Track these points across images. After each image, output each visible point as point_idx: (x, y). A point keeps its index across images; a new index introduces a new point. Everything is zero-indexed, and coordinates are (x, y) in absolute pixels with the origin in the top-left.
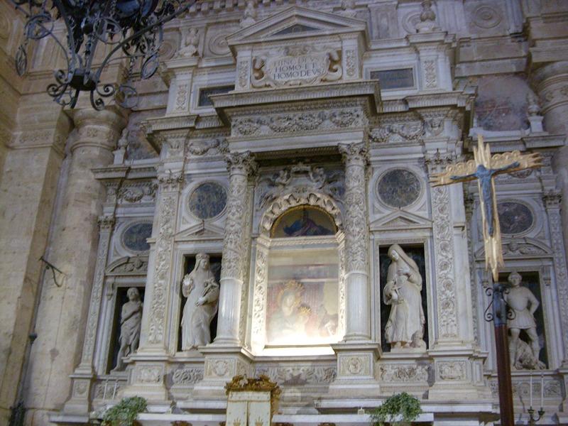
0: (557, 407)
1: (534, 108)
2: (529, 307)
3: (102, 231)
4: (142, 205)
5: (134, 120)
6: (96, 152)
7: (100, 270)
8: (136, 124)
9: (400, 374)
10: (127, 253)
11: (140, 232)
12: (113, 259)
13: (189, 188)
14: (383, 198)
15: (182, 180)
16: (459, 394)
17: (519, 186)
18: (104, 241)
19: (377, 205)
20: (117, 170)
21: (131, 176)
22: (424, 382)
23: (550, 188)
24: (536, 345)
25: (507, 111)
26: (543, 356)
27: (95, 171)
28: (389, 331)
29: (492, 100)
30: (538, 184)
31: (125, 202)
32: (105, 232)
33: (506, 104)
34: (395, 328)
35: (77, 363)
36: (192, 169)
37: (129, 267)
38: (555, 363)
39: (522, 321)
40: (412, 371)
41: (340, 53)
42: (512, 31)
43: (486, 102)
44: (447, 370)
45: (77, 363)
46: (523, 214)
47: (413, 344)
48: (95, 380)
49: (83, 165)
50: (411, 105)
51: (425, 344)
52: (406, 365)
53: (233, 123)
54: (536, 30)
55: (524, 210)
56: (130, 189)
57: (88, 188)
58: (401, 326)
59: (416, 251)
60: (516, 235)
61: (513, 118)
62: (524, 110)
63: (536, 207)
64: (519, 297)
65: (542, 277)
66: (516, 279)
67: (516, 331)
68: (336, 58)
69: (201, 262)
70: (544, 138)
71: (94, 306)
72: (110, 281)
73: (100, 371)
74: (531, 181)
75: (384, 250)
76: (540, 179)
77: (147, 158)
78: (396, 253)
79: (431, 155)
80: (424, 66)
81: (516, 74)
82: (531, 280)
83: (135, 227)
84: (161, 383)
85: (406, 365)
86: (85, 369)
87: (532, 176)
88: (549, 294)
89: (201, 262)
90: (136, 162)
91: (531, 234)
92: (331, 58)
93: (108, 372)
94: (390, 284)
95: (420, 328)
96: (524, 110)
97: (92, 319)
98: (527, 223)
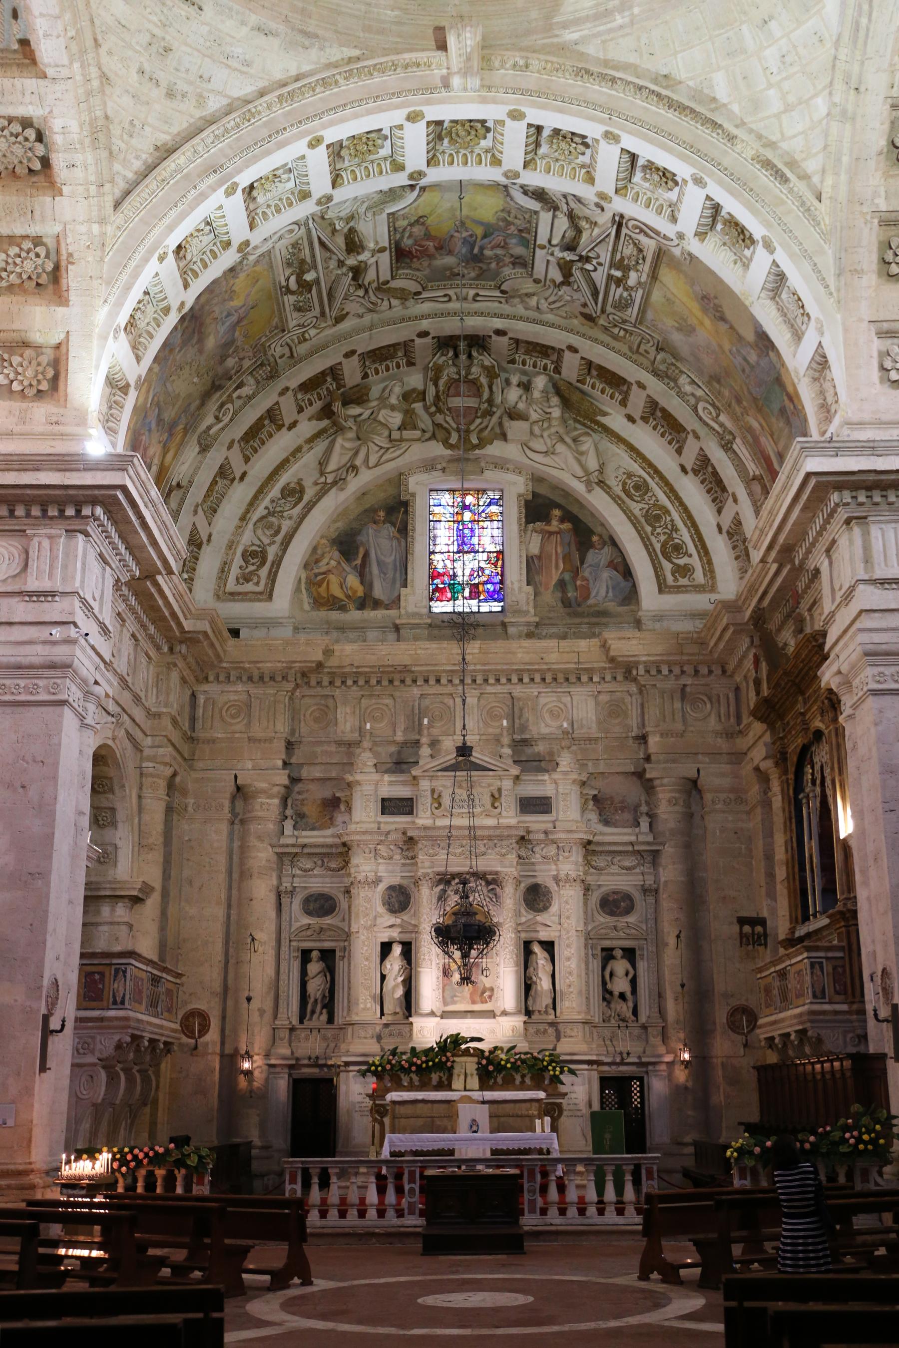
0: (641, 1050)
1: (644, 809)
2: (627, 974)
3: (283, 900)
4: (315, 876)
5: (298, 787)
6: (271, 826)
7: (285, 935)
8: (299, 793)
9: (537, 1032)
10: (306, 920)
11: (316, 900)
12: (295, 925)
13: (382, 887)
14: (527, 905)
15: (378, 881)
16: (576, 1049)
17: (625, 878)
18: (285, 908)
19: (523, 911)
20: (293, 845)
21: (306, 851)
22: (553, 1038)
23: (650, 881)
24: (631, 1004)
25: (623, 809)
26: (635, 1012)
27: (272, 846)
28: (530, 1003)
29: (612, 798)
30: (641, 877)
31: (298, 872)
32: (285, 900)
33: (622, 802)
34: (534, 1001)
35: (275, 1017)
36: (382, 871)
37: (309, 933)
38: (643, 1019)
39: (621, 985)
40: (545, 1031)
41: (500, 790)
42: (634, 734)
43: (607, 799)
44: (569, 1032)
45: (275, 1017)
46: (628, 902)
47: (546, 1012)
48: (292, 1029)
49: (260, 838)
50: (551, 837)
51: (553, 1012)
52: (542, 1027)
53: (420, 846)
54: (654, 741)
55: (628, 897)
56: (302, 860)
57: (268, 861)
58: (538, 1000)
59: (549, 946)
60: (620, 919)
61: (627, 816)
62: (637, 807)
63: (637, 896)
64: (620, 966)
65: (638, 953)
66: (618, 953)
67: (616, 993)
68: (497, 796)
69: (397, 950)
70: (649, 843)
71: (284, 965)
72: (294, 944)
73: (295, 1021)
74: (637, 874)
75: (527, 945)
76: (643, 874)
77: (313, 829)
78: (536, 948)
79: (562, 875)
80: (561, 798)
81: (633, 773)
82: (630, 954)
83: (311, 896)
84: (375, 1040)
85: (542, 1027)
86: (282, 1022)
87: (638, 870)
88: (642, 965)
89: (397, 950)
90: (305, 833)
91: (631, 919)
92: (493, 796)
93: (301, 1022)
94: (531, 970)
95: (550, 1001)
96: (637, 807)
97: (283, 977)
98: (629, 910)
